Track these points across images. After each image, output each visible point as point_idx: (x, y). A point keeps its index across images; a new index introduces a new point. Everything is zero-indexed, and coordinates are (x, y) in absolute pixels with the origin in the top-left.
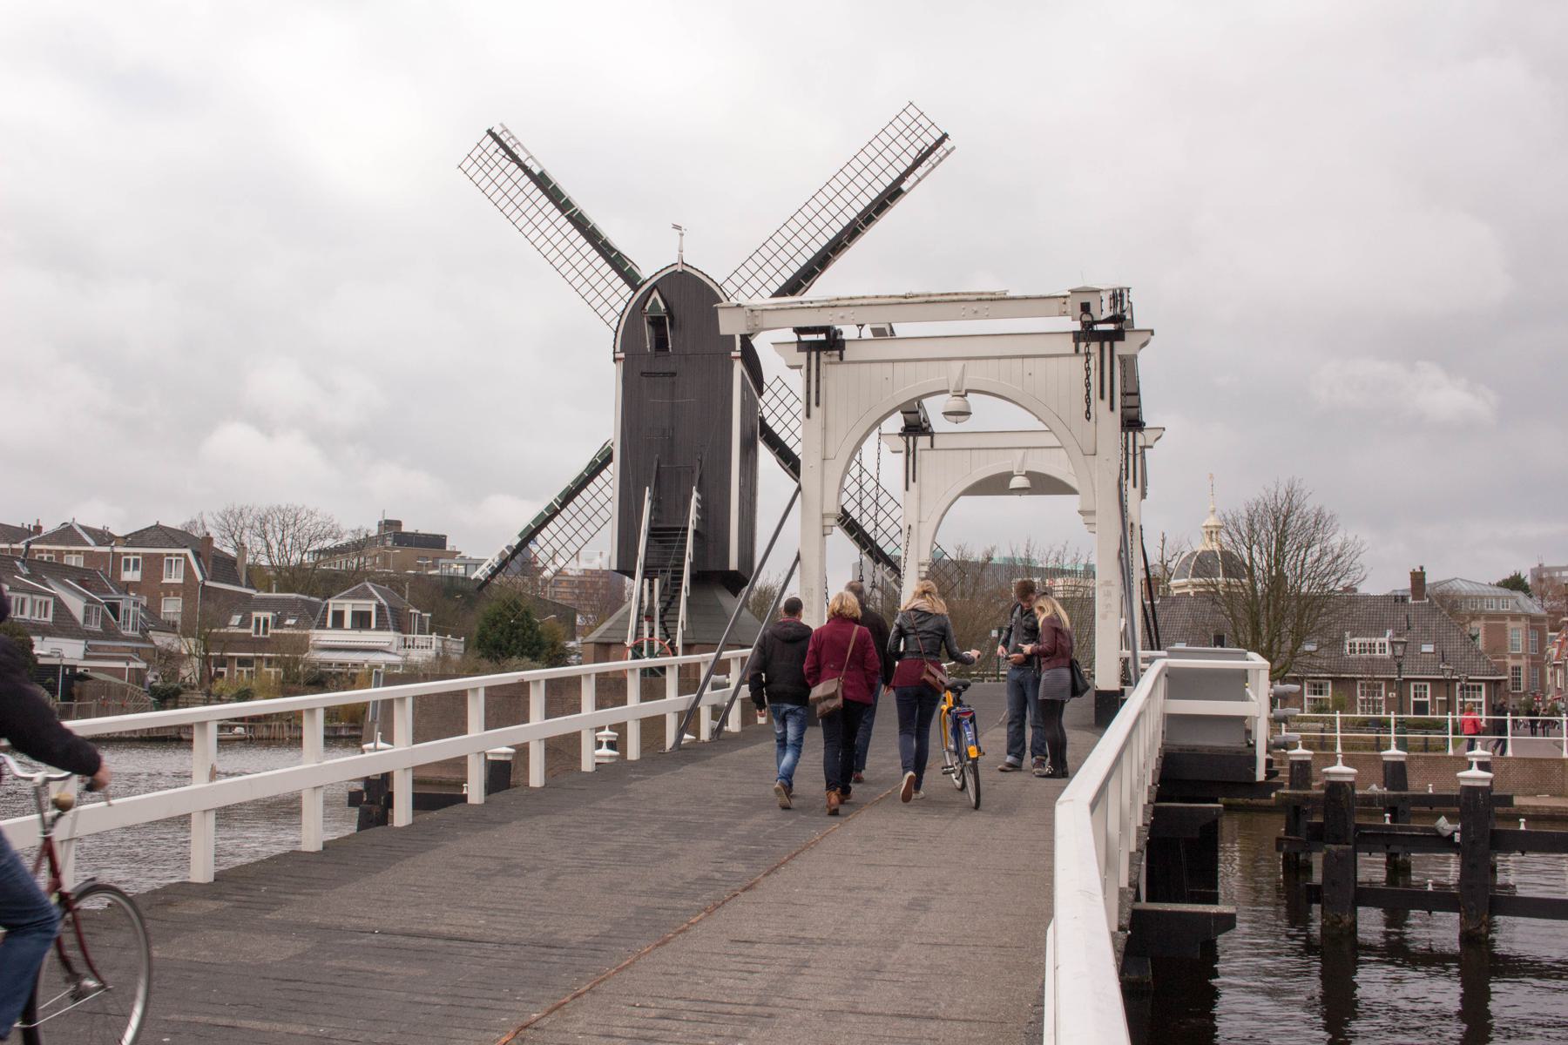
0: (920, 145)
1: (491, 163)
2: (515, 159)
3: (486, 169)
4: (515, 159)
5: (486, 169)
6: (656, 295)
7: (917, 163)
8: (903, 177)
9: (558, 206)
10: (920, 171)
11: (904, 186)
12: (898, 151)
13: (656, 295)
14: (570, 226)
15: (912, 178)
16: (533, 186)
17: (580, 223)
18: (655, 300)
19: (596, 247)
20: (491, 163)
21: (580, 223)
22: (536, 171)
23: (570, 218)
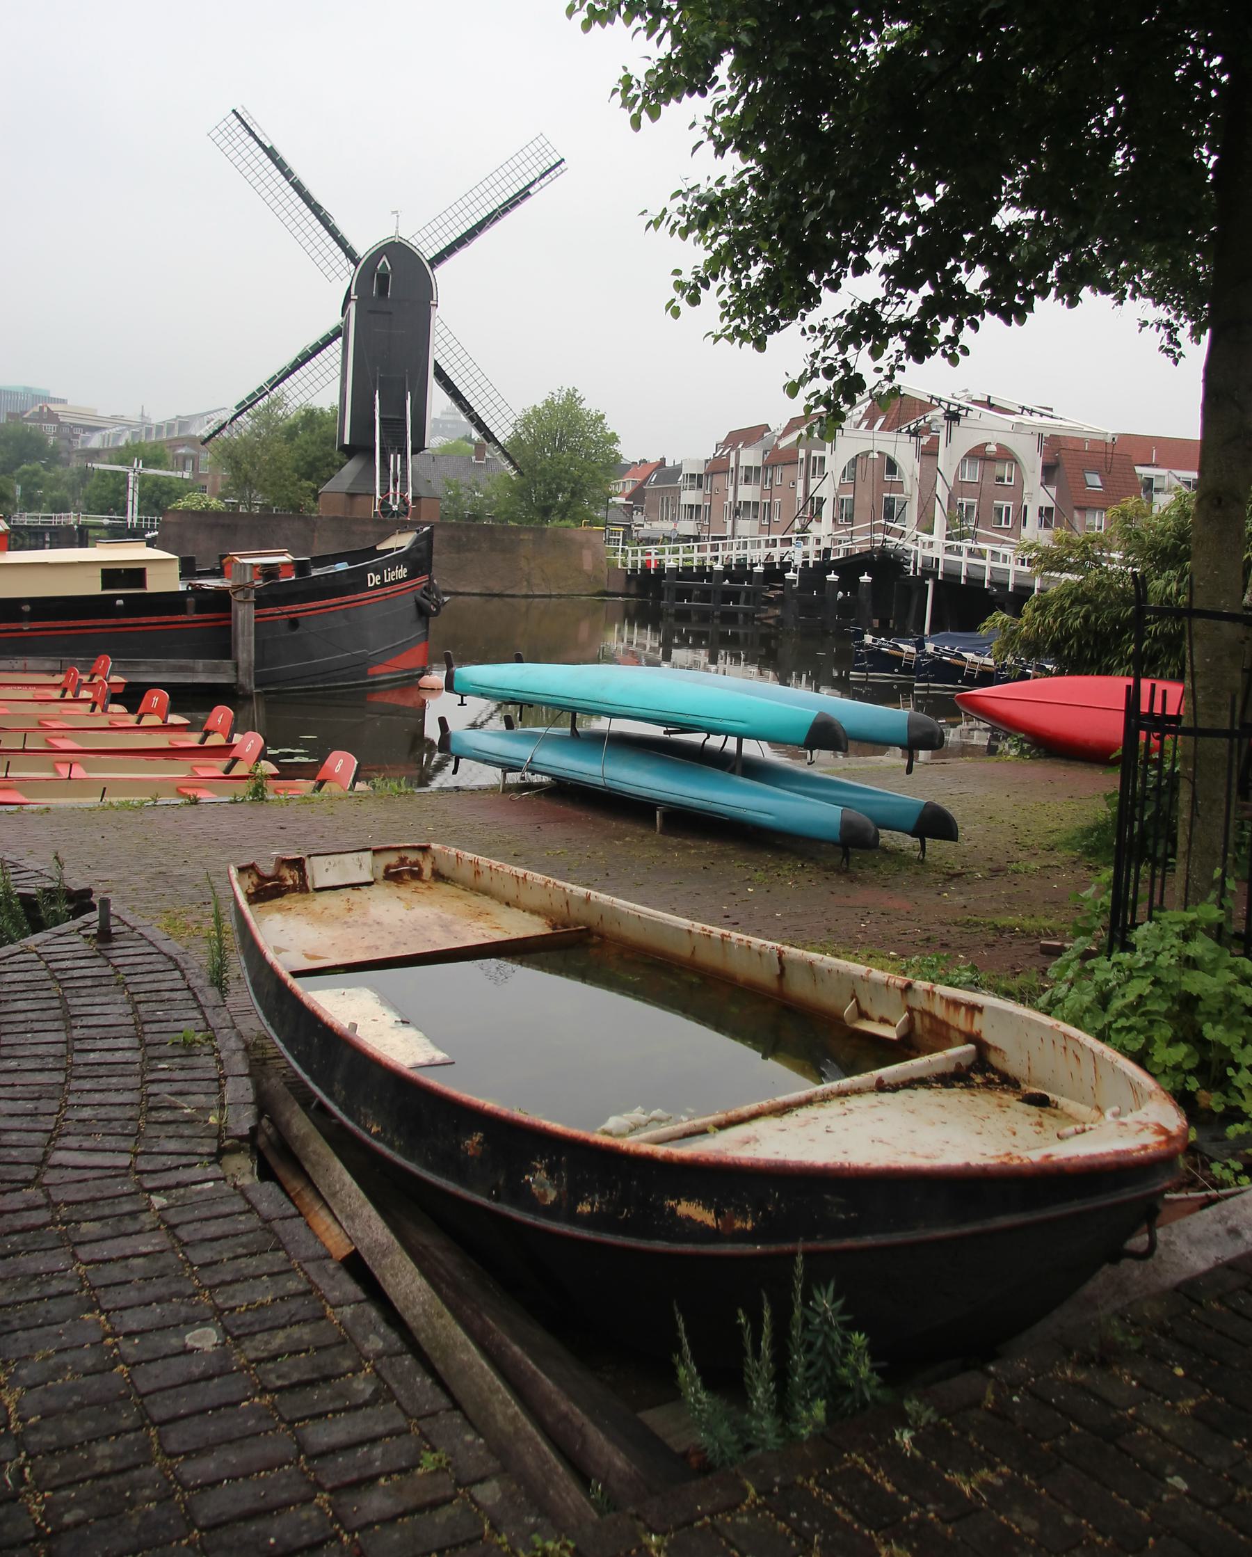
0: (545, 163)
1: (234, 135)
2: (252, 134)
3: (231, 139)
4: (252, 134)
5: (230, 139)
6: (384, 259)
7: (543, 176)
8: (532, 184)
9: (283, 173)
10: (543, 182)
11: (531, 190)
12: (530, 166)
13: (384, 259)
14: (291, 189)
15: (537, 186)
16: (265, 156)
17: (298, 187)
18: (384, 262)
19: (309, 206)
20: (234, 135)
21: (298, 187)
22: (268, 146)
23: (292, 184)
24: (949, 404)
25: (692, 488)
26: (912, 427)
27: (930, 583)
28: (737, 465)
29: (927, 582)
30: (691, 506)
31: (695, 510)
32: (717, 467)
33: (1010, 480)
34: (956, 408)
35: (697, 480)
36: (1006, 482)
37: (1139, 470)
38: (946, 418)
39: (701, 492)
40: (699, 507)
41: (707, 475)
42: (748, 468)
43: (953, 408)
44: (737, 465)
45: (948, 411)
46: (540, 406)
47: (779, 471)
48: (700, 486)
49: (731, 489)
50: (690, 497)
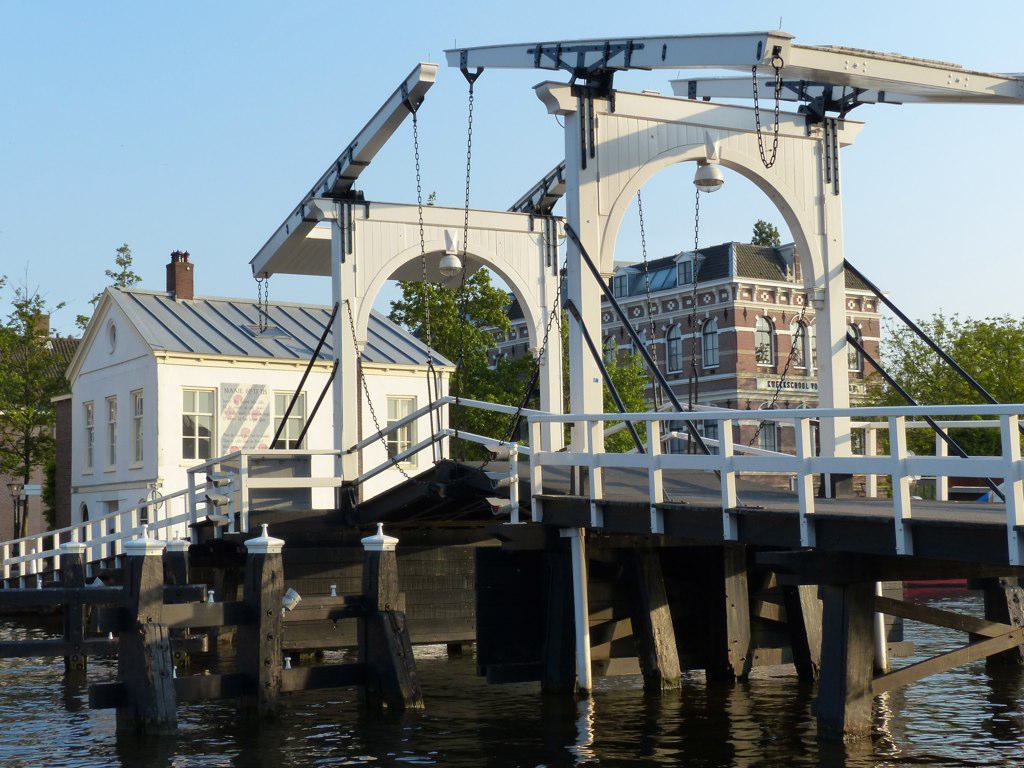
24: (581, 49)
29: (570, 533)
34: (599, 55)
43: (592, 59)
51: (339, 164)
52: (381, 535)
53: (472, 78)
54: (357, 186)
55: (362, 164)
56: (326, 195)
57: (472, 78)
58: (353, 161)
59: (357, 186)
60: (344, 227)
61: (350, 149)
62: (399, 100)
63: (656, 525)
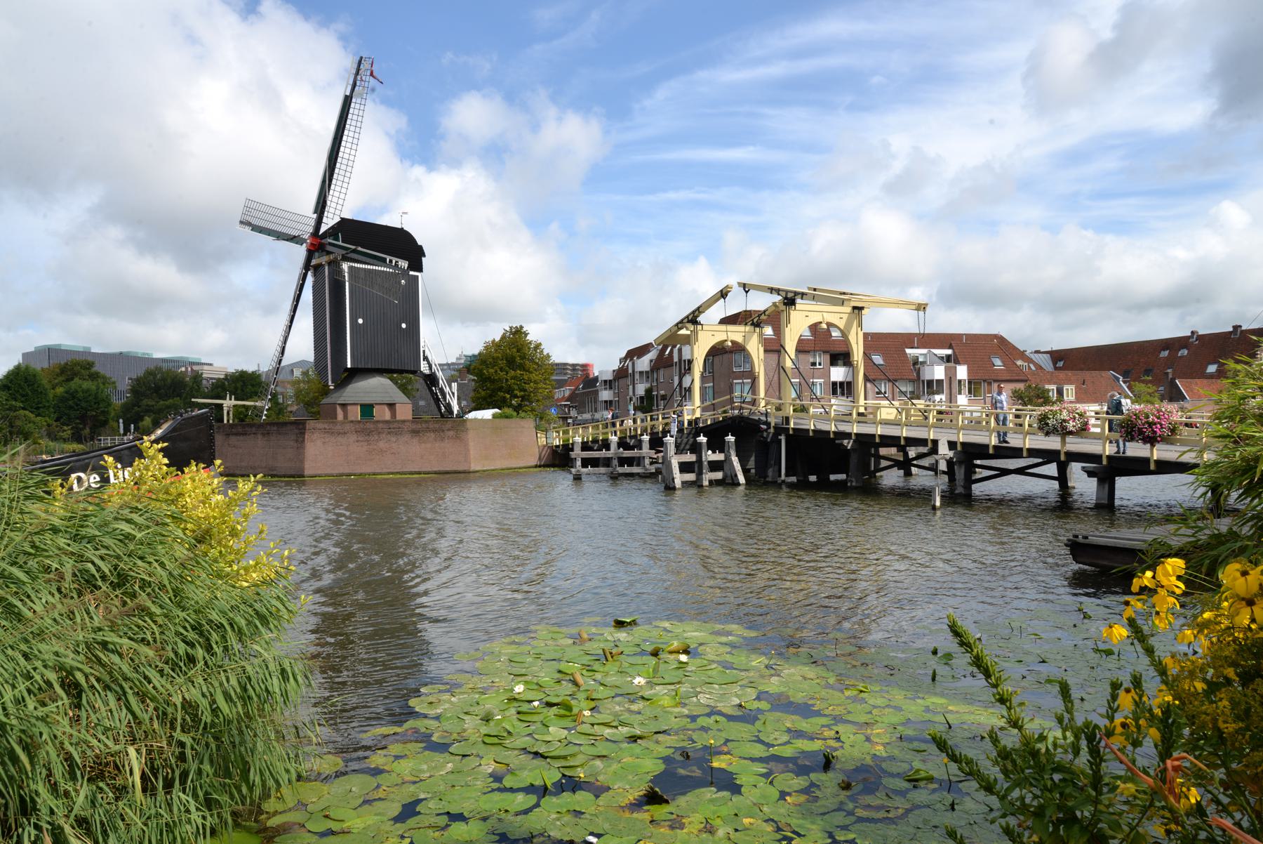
24: (787, 292)
25: (606, 389)
26: (755, 320)
27: (783, 438)
28: (633, 371)
30: (606, 402)
31: (608, 404)
32: (621, 374)
33: (820, 364)
34: (793, 295)
35: (609, 384)
36: (818, 367)
37: (908, 351)
38: (785, 304)
39: (612, 392)
40: (611, 402)
41: (614, 379)
42: (641, 373)
43: (790, 295)
44: (633, 371)
45: (786, 298)
46: (497, 339)
47: (661, 372)
48: (611, 388)
49: (631, 387)
50: (605, 395)
51: (693, 312)
52: (730, 437)
53: (747, 292)
54: (698, 319)
55: (700, 313)
56: (688, 322)
57: (747, 292)
58: (699, 311)
59: (698, 319)
60: (695, 332)
61: (699, 308)
62: (720, 295)
63: (811, 434)
